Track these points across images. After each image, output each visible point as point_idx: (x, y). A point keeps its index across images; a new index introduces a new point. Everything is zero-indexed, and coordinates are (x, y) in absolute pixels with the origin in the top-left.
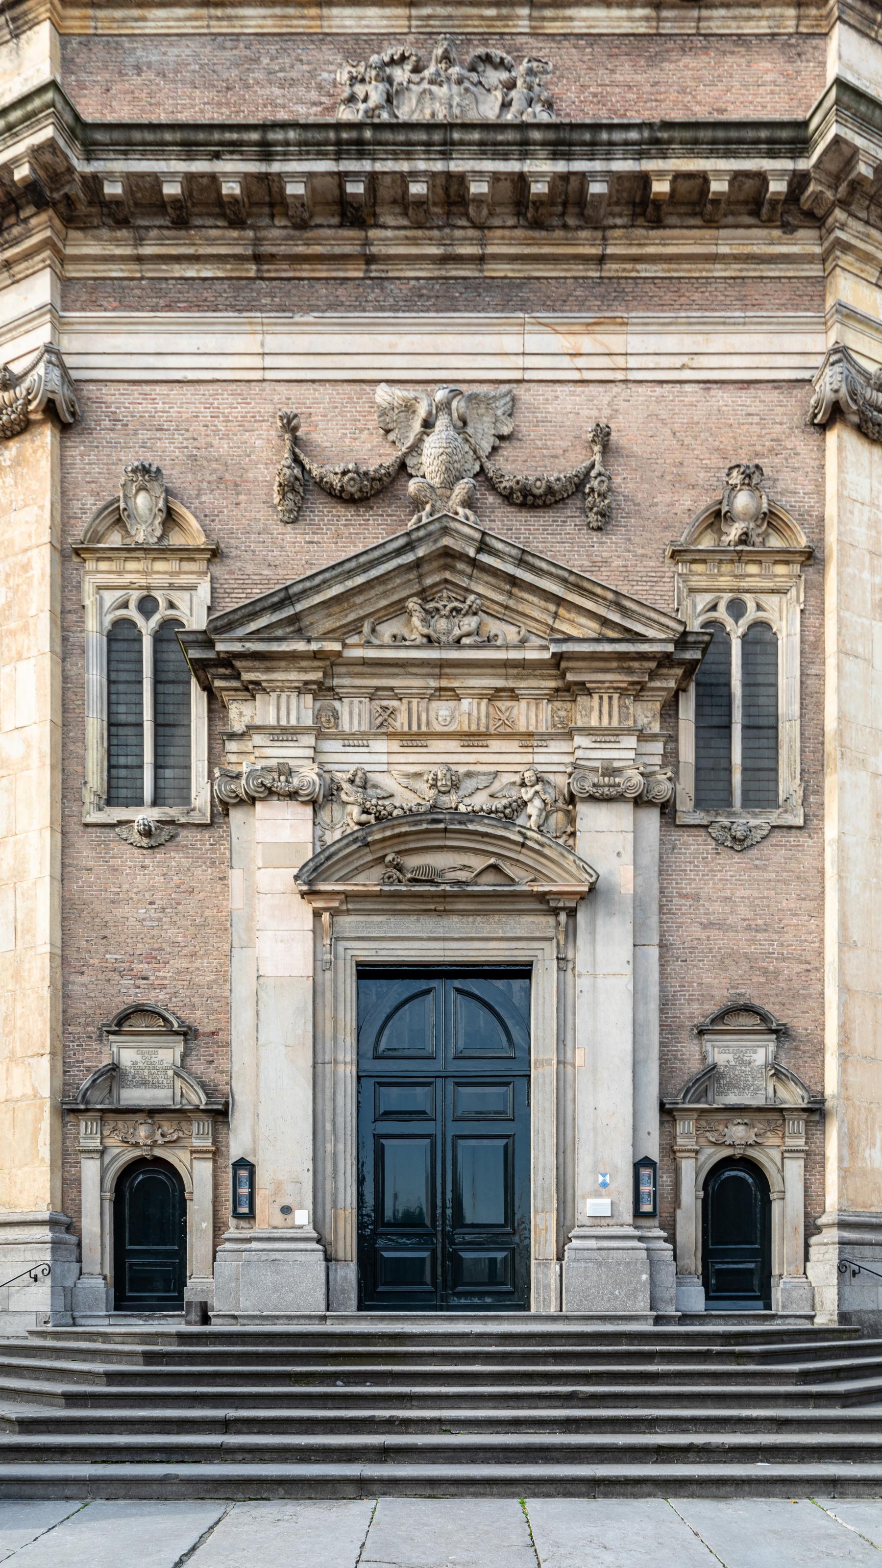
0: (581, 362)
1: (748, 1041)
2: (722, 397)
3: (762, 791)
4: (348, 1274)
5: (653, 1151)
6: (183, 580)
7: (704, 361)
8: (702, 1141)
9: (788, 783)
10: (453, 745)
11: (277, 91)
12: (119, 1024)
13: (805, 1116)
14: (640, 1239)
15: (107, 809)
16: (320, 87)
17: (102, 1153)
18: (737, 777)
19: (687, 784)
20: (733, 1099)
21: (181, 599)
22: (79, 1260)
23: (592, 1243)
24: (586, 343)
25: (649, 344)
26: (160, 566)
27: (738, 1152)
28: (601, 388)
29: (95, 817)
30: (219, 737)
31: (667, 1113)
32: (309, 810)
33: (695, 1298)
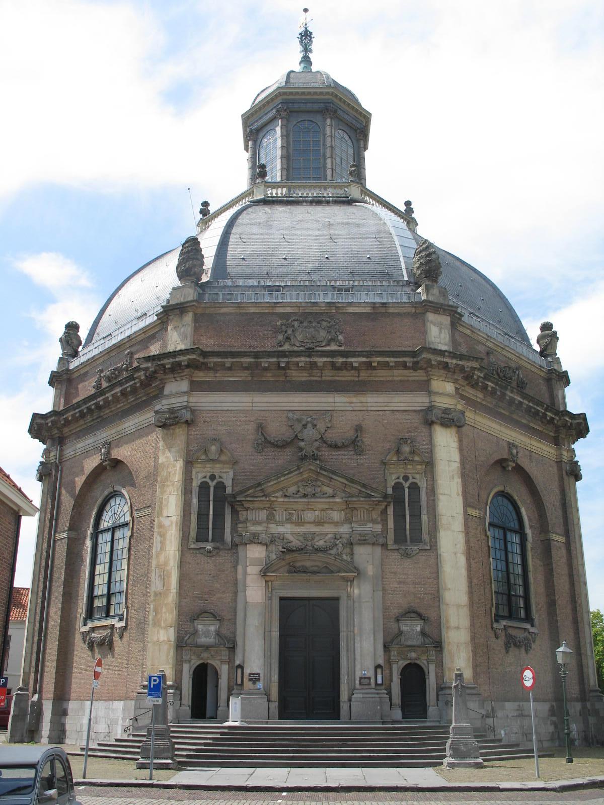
0: (353, 405)
1: (414, 623)
2: (398, 415)
3: (417, 539)
4: (275, 706)
5: (381, 661)
6: (225, 470)
7: (392, 405)
8: (399, 658)
9: (425, 536)
10: (312, 526)
12: (198, 617)
13: (435, 648)
14: (378, 694)
15: (197, 543)
16: (272, 326)
17: (190, 662)
18: (408, 532)
19: (391, 536)
20: (410, 643)
21: (224, 476)
22: (181, 700)
23: (360, 695)
24: (354, 400)
25: (373, 400)
26: (218, 466)
27: (413, 662)
28: (359, 412)
29: (192, 546)
30: (235, 522)
31: (386, 648)
32: (264, 548)
33: (398, 714)
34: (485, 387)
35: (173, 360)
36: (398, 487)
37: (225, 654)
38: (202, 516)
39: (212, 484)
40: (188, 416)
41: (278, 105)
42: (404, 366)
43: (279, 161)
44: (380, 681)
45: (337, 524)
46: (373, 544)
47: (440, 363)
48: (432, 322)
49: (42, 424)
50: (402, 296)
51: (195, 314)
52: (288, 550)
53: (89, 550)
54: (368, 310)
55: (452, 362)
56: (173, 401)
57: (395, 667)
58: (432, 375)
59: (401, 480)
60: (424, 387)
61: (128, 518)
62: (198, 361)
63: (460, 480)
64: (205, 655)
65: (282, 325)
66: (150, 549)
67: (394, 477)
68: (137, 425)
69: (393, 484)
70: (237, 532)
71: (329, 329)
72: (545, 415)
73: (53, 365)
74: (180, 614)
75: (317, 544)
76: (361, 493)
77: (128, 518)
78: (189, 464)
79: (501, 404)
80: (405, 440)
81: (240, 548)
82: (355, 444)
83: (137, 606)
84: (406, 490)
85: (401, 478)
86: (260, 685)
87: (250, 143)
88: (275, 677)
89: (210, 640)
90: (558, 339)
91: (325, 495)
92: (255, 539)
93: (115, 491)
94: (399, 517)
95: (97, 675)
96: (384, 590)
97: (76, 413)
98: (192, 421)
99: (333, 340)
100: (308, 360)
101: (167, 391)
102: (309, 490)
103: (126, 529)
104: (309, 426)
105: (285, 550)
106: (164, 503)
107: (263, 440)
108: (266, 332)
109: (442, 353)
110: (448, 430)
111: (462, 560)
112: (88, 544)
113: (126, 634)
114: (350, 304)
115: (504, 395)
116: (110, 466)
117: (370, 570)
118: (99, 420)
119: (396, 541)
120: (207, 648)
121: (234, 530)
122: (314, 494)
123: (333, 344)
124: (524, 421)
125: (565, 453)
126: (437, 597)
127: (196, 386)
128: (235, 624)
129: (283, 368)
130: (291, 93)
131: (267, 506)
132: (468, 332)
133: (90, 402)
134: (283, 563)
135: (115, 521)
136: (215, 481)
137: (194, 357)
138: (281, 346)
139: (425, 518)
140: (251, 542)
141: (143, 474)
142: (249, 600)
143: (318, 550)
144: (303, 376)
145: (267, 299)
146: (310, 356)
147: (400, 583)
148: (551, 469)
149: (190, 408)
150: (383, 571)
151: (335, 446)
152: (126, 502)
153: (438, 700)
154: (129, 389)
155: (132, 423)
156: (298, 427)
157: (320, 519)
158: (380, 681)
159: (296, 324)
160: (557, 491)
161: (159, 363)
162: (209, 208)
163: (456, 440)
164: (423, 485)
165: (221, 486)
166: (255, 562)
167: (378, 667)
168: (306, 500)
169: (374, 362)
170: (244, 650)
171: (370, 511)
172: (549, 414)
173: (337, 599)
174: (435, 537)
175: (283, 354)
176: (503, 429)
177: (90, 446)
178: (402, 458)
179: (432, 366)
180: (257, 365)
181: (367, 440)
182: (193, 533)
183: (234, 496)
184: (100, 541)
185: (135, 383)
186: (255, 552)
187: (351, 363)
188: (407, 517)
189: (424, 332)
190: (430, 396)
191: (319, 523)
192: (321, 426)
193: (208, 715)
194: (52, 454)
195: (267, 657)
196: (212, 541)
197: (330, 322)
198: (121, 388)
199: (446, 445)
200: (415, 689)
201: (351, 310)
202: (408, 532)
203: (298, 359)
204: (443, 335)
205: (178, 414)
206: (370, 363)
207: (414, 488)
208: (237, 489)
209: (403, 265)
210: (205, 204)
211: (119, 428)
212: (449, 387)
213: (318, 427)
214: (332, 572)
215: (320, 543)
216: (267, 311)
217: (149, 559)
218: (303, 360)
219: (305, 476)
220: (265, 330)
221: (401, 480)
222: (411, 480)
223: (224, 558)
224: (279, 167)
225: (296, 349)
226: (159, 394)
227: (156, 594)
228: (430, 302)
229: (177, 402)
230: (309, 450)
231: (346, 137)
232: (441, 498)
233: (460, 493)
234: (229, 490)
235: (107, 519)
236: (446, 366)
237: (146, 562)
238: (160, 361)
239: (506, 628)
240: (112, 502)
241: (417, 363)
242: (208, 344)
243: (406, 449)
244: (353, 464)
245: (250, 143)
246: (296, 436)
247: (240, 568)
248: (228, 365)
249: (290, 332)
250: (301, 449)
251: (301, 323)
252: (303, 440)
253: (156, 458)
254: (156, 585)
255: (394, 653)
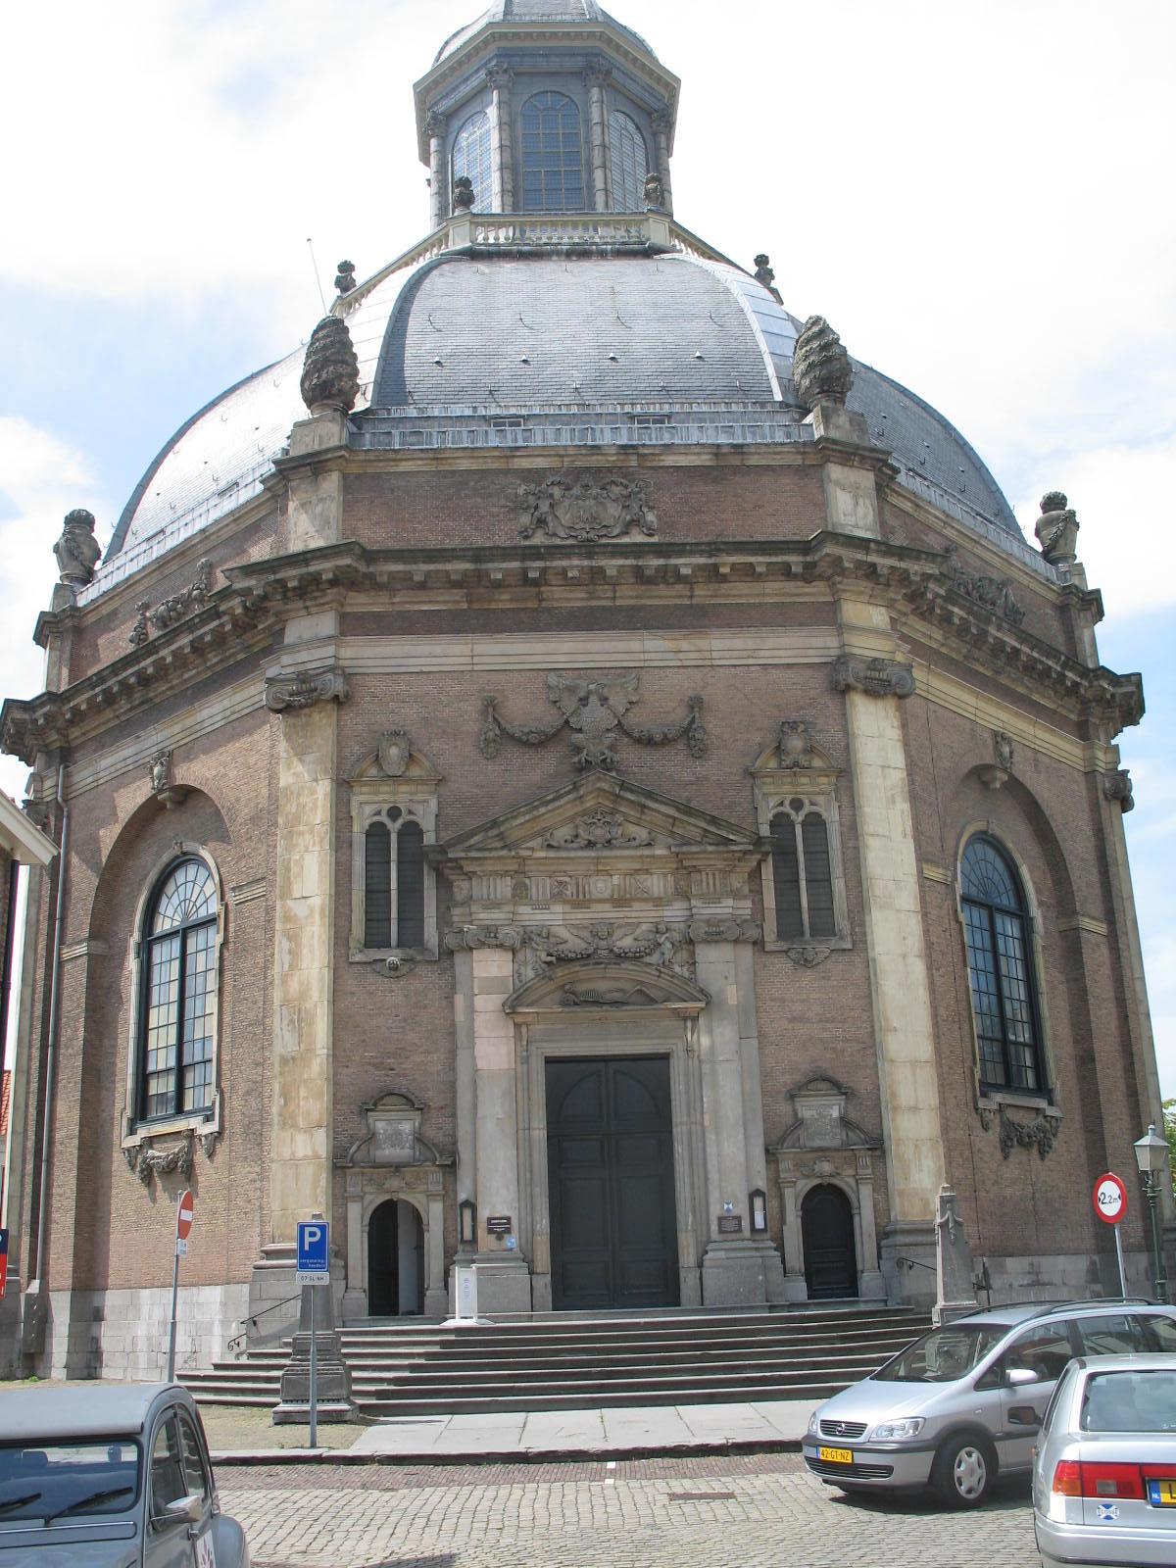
1: (825, 1101)
2: (775, 674)
3: (824, 928)
4: (544, 1283)
5: (761, 1183)
6: (420, 797)
8: (798, 1174)
9: (842, 922)
10: (607, 906)
11: (479, 500)
12: (375, 1105)
13: (870, 1153)
14: (757, 1249)
15: (366, 951)
16: (507, 498)
17: (362, 1198)
20: (818, 1143)
21: (419, 809)
22: (346, 1278)
23: (722, 1254)
24: (685, 645)
25: (724, 646)
26: (404, 788)
27: (827, 1181)
28: (696, 670)
29: (358, 958)
31: (771, 1154)
33: (799, 1289)
34: (947, 618)
35: (304, 570)
36: (780, 822)
37: (435, 1178)
38: (375, 893)
39: (394, 827)
40: (338, 686)
41: (489, 61)
42: (786, 572)
43: (496, 176)
44: (759, 1223)
45: (658, 902)
46: (736, 941)
47: (859, 564)
48: (838, 483)
49: (24, 721)
50: (774, 431)
51: (345, 477)
52: (559, 959)
53: (134, 978)
54: (705, 460)
55: (884, 563)
56: (304, 656)
57: (789, 1193)
58: (845, 591)
59: (787, 809)
60: (828, 615)
61: (214, 907)
62: (357, 571)
63: (907, 806)
64: (394, 1183)
65: (527, 493)
66: (267, 967)
67: (773, 801)
68: (228, 713)
69: (770, 816)
70: (450, 924)
71: (625, 502)
72: (1062, 677)
73: (43, 601)
74: (336, 1101)
75: (619, 944)
76: (705, 834)
77: (214, 907)
78: (343, 786)
79: (977, 653)
80: (793, 726)
81: (459, 959)
82: (689, 737)
83: (242, 1088)
84: (799, 830)
85: (787, 803)
86: (512, 1241)
87: (433, 142)
88: (543, 1224)
89: (403, 1152)
90: (1077, 525)
91: (633, 843)
92: (490, 939)
93: (185, 854)
94: (787, 884)
95: (184, 1229)
96: (761, 1035)
97: (96, 695)
98: (347, 696)
99: (635, 522)
100: (586, 563)
101: (291, 635)
102: (599, 832)
103: (212, 930)
104: (594, 700)
105: (553, 959)
106: (294, 869)
107: (498, 732)
108: (495, 510)
109: (862, 544)
110: (880, 704)
111: (918, 969)
112: (132, 965)
113: (222, 1149)
114: (668, 448)
115: (984, 633)
116: (173, 802)
117: (732, 995)
118: (146, 706)
119: (781, 935)
120: (397, 1167)
121: (444, 920)
122: (609, 842)
123: (635, 531)
124: (1020, 690)
125: (1100, 755)
126: (870, 1045)
127: (352, 625)
128: (454, 1115)
129: (535, 583)
130: (516, 35)
131: (511, 868)
132: (907, 506)
133: (125, 670)
134: (551, 986)
135: (186, 916)
136: (400, 821)
137: (347, 561)
138: (526, 538)
139: (838, 885)
140: (482, 945)
141: (245, 812)
142: (481, 1064)
143: (622, 957)
144: (573, 599)
145: (494, 441)
146: (590, 556)
147: (793, 1020)
148: (1075, 787)
149: (343, 668)
150: (757, 997)
151: (648, 742)
152: (210, 874)
153: (879, 1257)
154: (208, 638)
155: (217, 708)
156: (570, 704)
157: (627, 894)
158: (759, 1223)
159: (557, 492)
160: (1088, 831)
161: (272, 577)
162: (354, 275)
163: (896, 723)
164: (832, 817)
165: (412, 831)
166: (492, 985)
167: (757, 1193)
168: (593, 854)
169: (724, 565)
170: (476, 1169)
171: (726, 873)
172: (1069, 674)
173: (665, 1057)
174: (863, 924)
175: (535, 553)
176: (981, 705)
177: (129, 761)
178: (788, 761)
179: (843, 572)
180: (480, 577)
181: (713, 726)
182: (358, 930)
183: (442, 849)
184: (156, 958)
185: (222, 625)
186: (491, 966)
187: (676, 568)
188: (803, 884)
189: (823, 505)
190: (840, 634)
191: (620, 901)
192: (618, 701)
193: (402, 1307)
194: (48, 783)
195: (524, 1180)
196: (399, 945)
197: (626, 487)
198: (191, 637)
199: (876, 734)
200: (829, 1237)
201: (670, 460)
202: (806, 916)
203: (564, 563)
204: (861, 511)
205: (318, 683)
206: (716, 567)
207: (815, 823)
208: (447, 835)
209: (771, 371)
210: (346, 268)
211: (188, 722)
212: (879, 617)
213: (611, 701)
214: (653, 1001)
215: (627, 943)
216: (495, 466)
217: (266, 988)
218: (575, 565)
219: (590, 803)
220: (494, 506)
221: (787, 809)
222: (807, 808)
223: (426, 978)
224: (496, 187)
225: (558, 542)
226: (274, 644)
227: (284, 1061)
228: (834, 442)
229: (313, 658)
230: (594, 750)
231: (631, 127)
232: (871, 842)
233: (909, 831)
234: (429, 839)
235: (170, 912)
236: (871, 572)
237: (259, 996)
238: (274, 573)
239: (1001, 1108)
240: (180, 877)
241: (814, 565)
242: (375, 534)
243: (796, 743)
244: (687, 776)
245: (433, 142)
246: (567, 722)
247: (459, 1000)
248: (417, 578)
249: (544, 507)
250: (578, 749)
251: (568, 489)
252: (580, 730)
253: (273, 778)
254: (284, 1040)
255: (786, 1165)
